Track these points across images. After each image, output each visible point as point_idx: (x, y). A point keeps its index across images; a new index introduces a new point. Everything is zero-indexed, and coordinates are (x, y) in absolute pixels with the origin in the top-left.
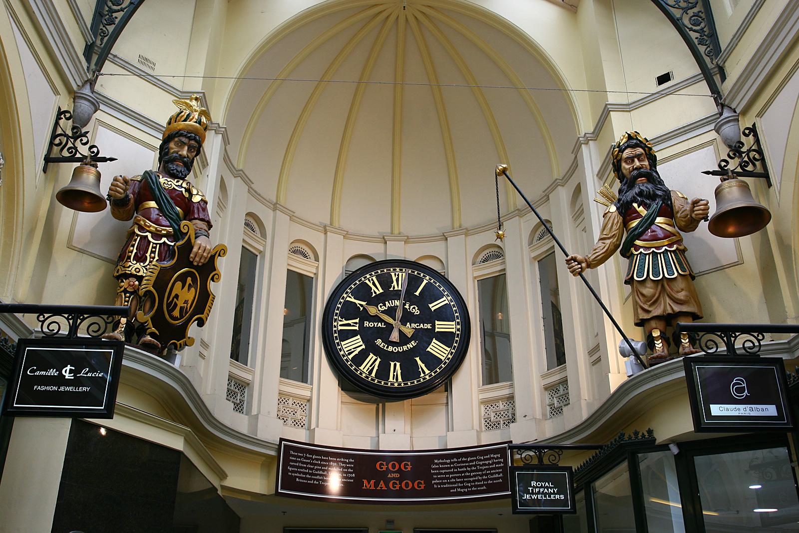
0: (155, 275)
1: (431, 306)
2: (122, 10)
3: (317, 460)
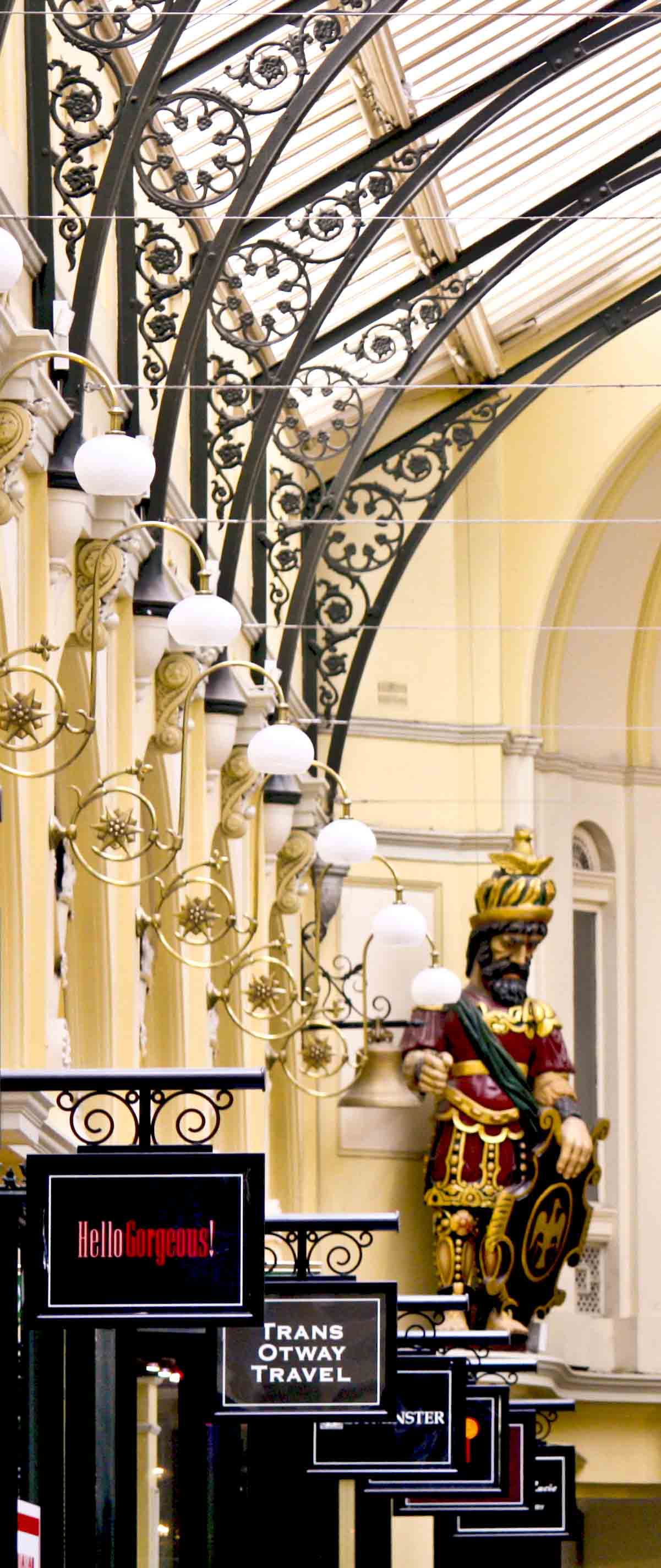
2: (353, 633)
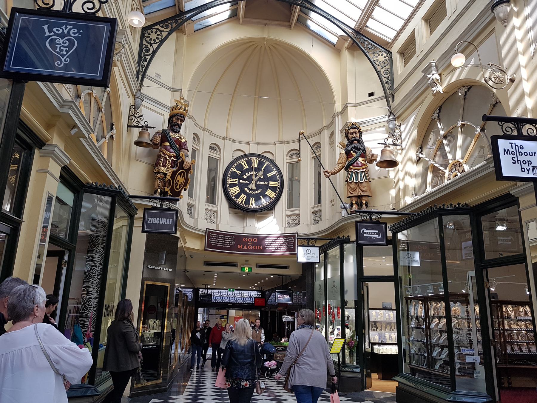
0: (171, 174)
1: (268, 175)
2: (149, 55)
3: (220, 236)
